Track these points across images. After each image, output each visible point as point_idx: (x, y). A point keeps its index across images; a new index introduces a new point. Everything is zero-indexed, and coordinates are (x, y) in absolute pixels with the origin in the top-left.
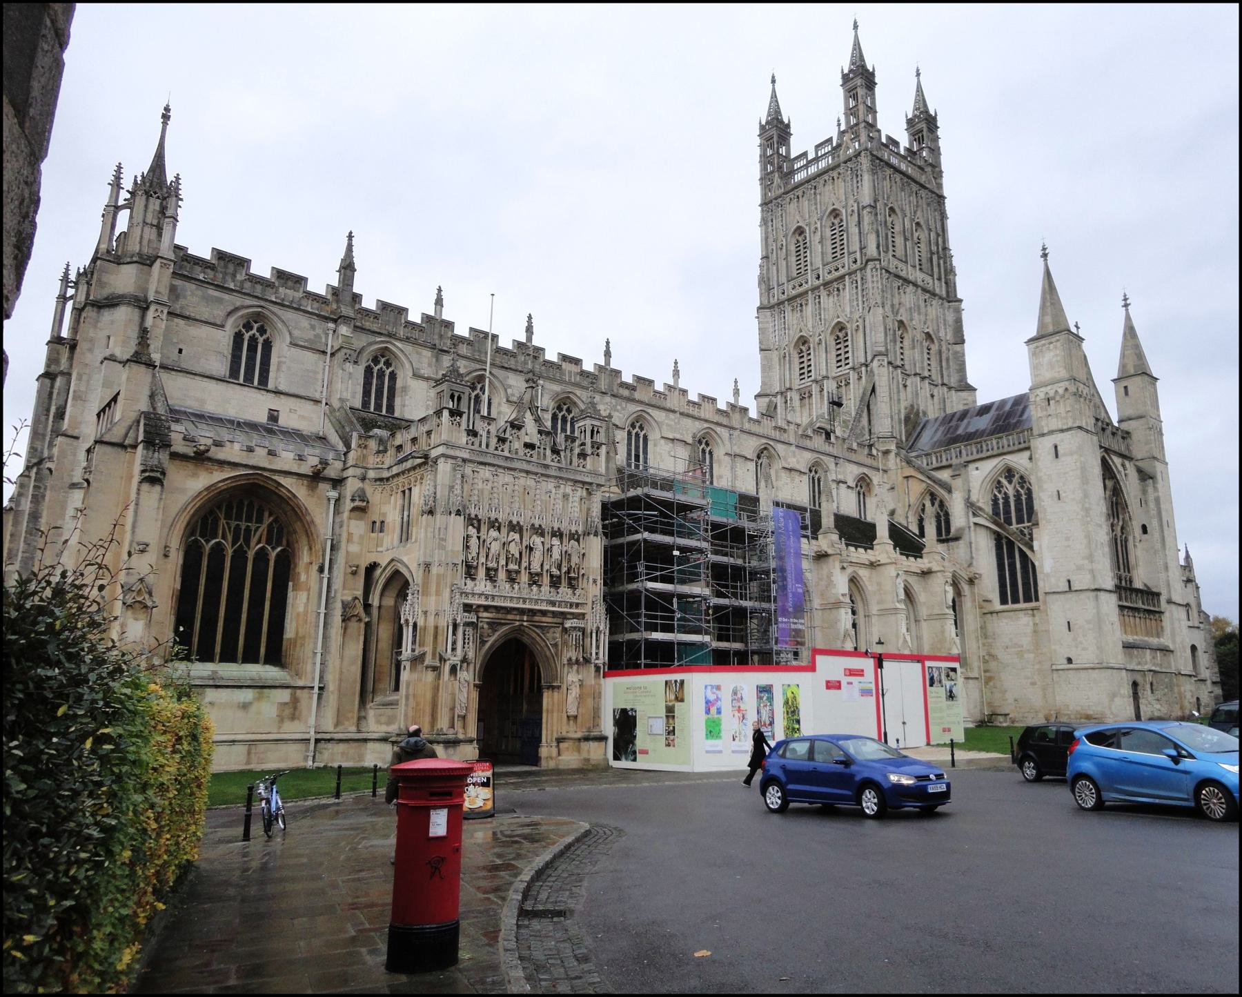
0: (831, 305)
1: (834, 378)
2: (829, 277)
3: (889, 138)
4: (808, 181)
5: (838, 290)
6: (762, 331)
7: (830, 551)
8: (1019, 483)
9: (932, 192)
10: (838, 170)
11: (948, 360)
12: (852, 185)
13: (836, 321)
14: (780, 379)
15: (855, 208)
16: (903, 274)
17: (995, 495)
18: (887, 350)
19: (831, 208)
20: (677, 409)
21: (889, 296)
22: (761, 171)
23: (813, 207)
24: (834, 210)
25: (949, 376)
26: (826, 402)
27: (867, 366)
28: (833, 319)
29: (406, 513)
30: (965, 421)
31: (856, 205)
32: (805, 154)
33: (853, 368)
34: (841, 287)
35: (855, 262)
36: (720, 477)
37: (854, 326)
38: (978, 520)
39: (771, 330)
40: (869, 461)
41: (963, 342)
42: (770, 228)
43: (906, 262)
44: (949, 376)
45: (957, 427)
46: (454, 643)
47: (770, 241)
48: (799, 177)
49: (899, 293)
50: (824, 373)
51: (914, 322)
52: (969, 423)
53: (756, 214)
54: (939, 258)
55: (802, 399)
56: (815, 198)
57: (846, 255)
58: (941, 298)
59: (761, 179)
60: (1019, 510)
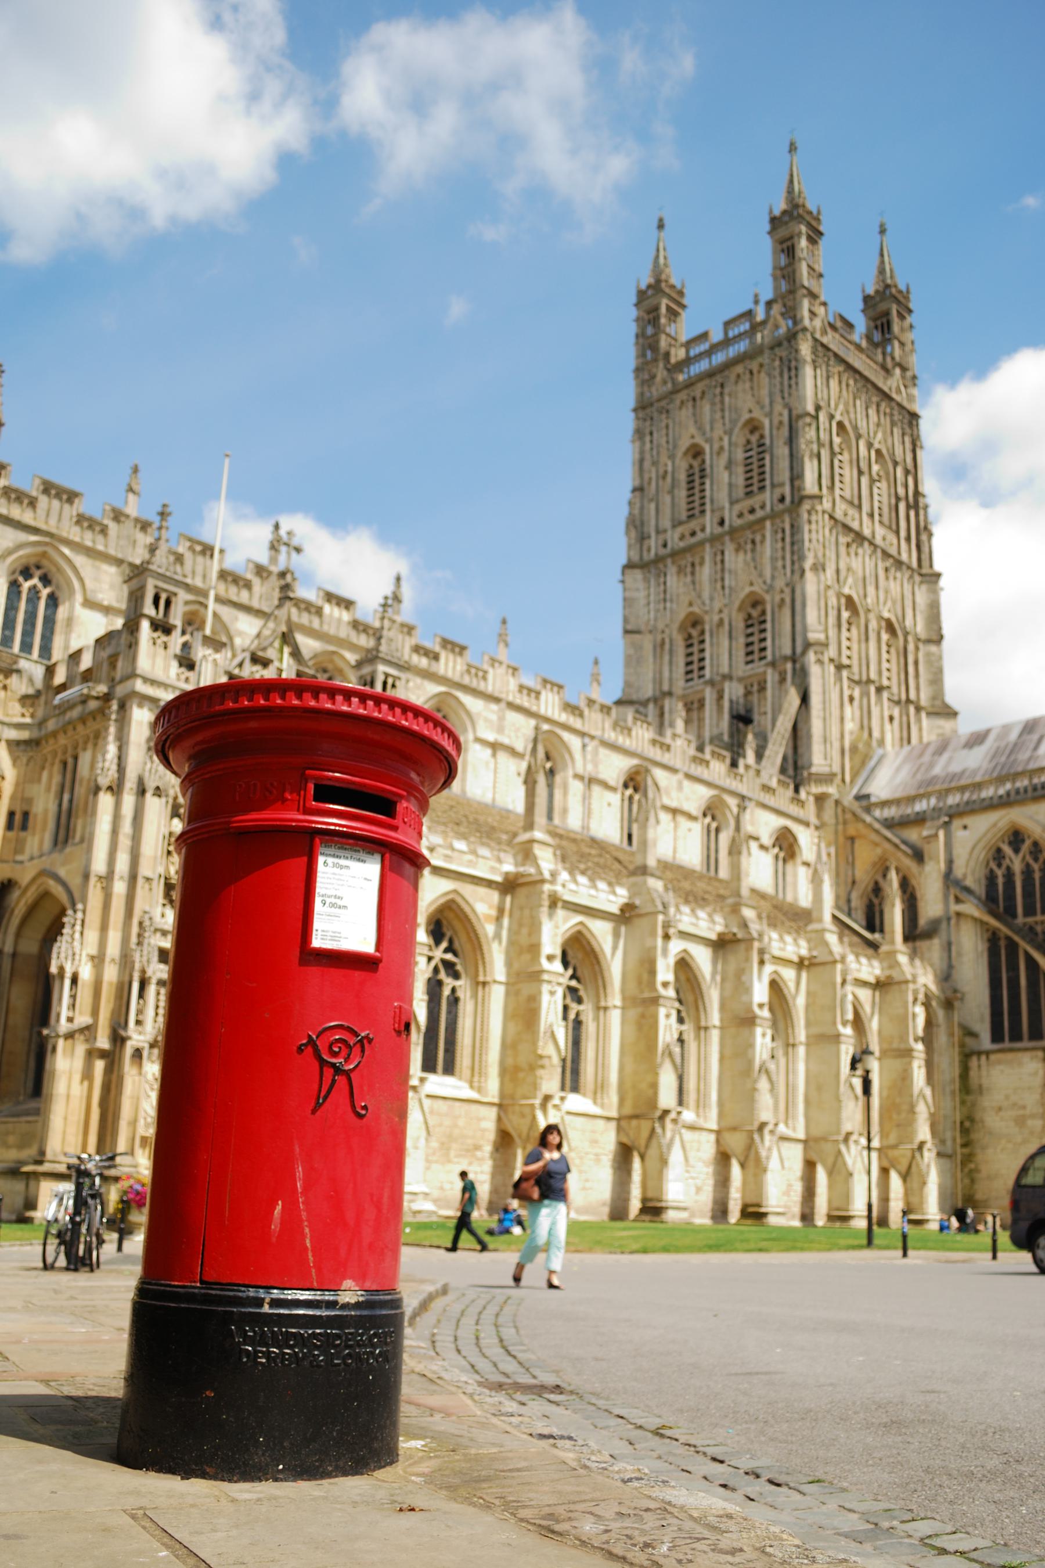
1: (740, 680)
2: (739, 522)
4: (710, 374)
5: (753, 542)
6: (628, 602)
7: (740, 936)
8: (1031, 853)
9: (900, 406)
10: (760, 360)
11: (916, 663)
12: (782, 384)
14: (654, 681)
15: (785, 419)
16: (855, 525)
17: (992, 871)
18: (827, 637)
19: (746, 416)
20: (503, 696)
21: (833, 557)
22: (638, 357)
23: (718, 415)
24: (751, 421)
25: (918, 689)
26: (726, 716)
27: (794, 659)
28: (743, 589)
29: (66, 797)
30: (945, 756)
31: (786, 413)
33: (773, 664)
34: (758, 538)
35: (782, 499)
36: (565, 811)
37: (777, 598)
38: (960, 908)
39: (643, 602)
40: (794, 810)
42: (648, 446)
43: (859, 507)
44: (918, 689)
45: (931, 765)
46: (140, 1012)
47: (647, 464)
49: (848, 554)
50: (725, 669)
52: (951, 759)
53: (628, 422)
54: (908, 507)
56: (722, 402)
57: (768, 488)
58: (909, 567)
59: (638, 370)
60: (1028, 893)
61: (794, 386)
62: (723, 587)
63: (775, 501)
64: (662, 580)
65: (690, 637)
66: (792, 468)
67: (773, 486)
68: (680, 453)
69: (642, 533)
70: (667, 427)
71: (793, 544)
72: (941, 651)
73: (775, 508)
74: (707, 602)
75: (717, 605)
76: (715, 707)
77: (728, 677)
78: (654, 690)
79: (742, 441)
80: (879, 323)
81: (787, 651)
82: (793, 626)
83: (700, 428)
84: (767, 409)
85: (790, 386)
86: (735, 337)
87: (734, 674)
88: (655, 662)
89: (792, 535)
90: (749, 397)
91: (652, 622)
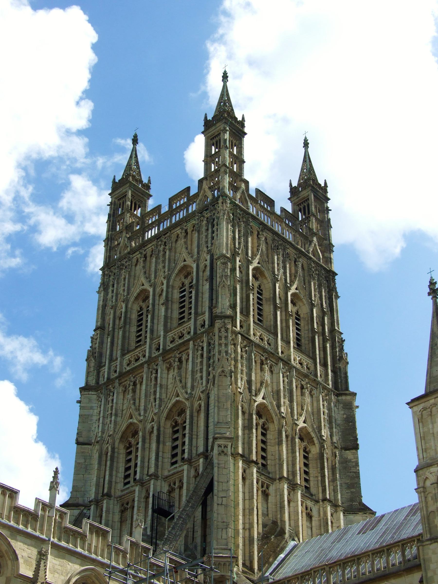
0: (170, 381)
1: (166, 478)
3: (258, 191)
5: (180, 361)
12: (207, 236)
13: (173, 401)
14: (97, 485)
22: (108, 231)
32: (159, 208)
33: (190, 461)
34: (184, 357)
37: (196, 405)
39: (95, 418)
41: (356, 447)
44: (335, 491)
47: (108, 309)
48: (149, 234)
51: (282, 410)
54: (324, 341)
55: (123, 512)
57: (193, 316)
58: (324, 388)
61: (215, 238)
62: (155, 399)
63: (199, 327)
64: (111, 398)
65: (130, 446)
66: (211, 299)
67: (196, 313)
68: (132, 299)
69: (100, 362)
70: (125, 279)
71: (209, 358)
72: (357, 458)
73: (199, 332)
74: (142, 413)
75: (150, 416)
76: (143, 505)
77: (155, 476)
78: (97, 493)
79: (178, 284)
80: (302, 207)
81: (201, 449)
82: (207, 426)
83: (148, 278)
84: (195, 257)
85: (213, 238)
86: (177, 208)
87: (160, 473)
88: (99, 469)
89: (209, 351)
90: (184, 249)
91: (100, 434)
